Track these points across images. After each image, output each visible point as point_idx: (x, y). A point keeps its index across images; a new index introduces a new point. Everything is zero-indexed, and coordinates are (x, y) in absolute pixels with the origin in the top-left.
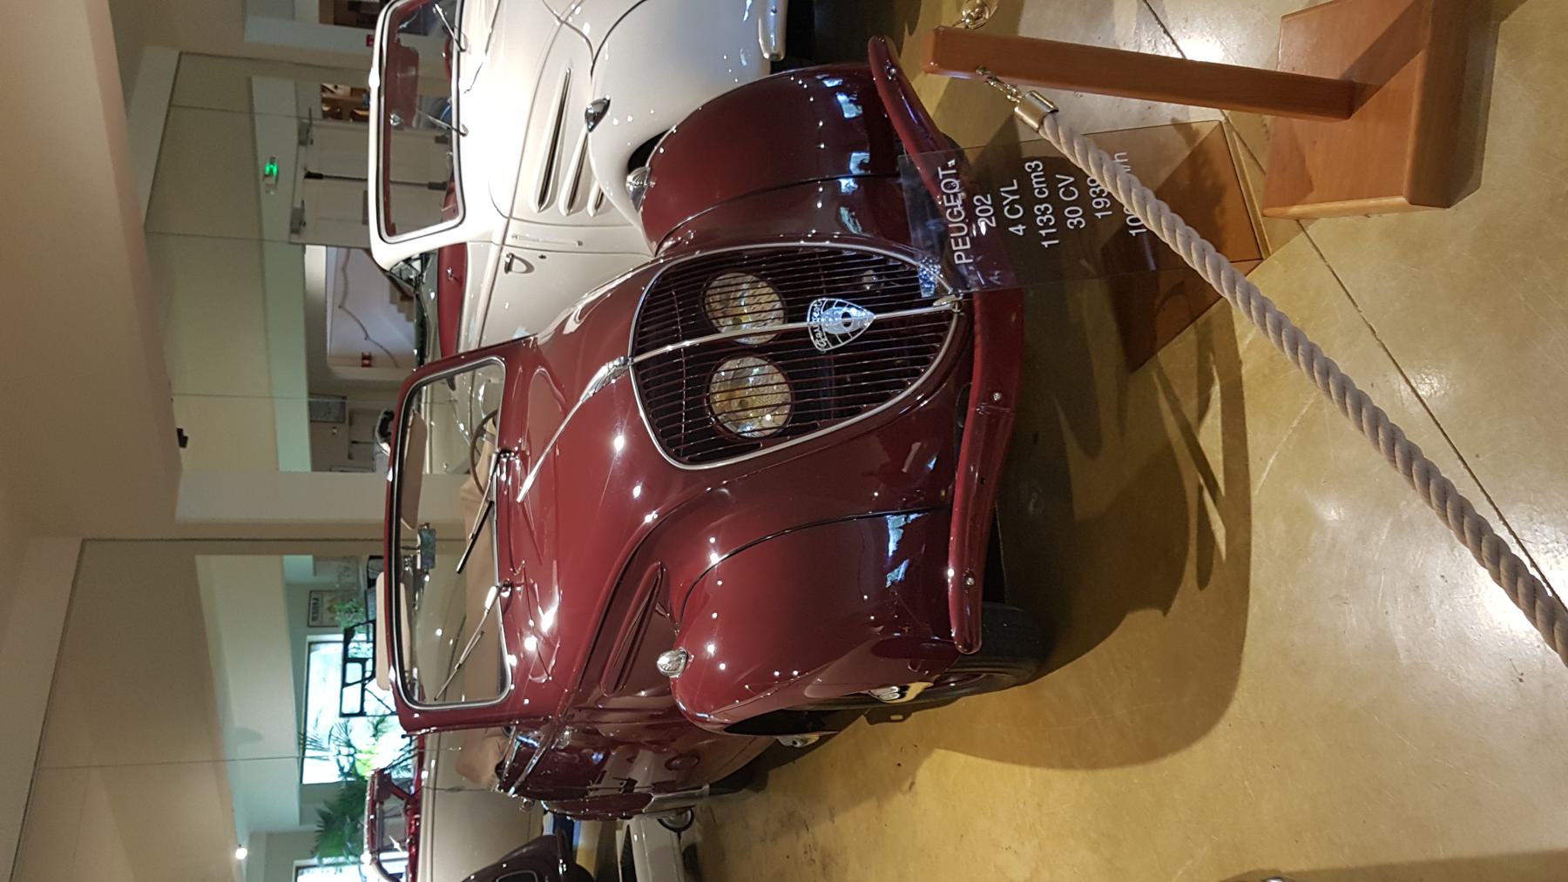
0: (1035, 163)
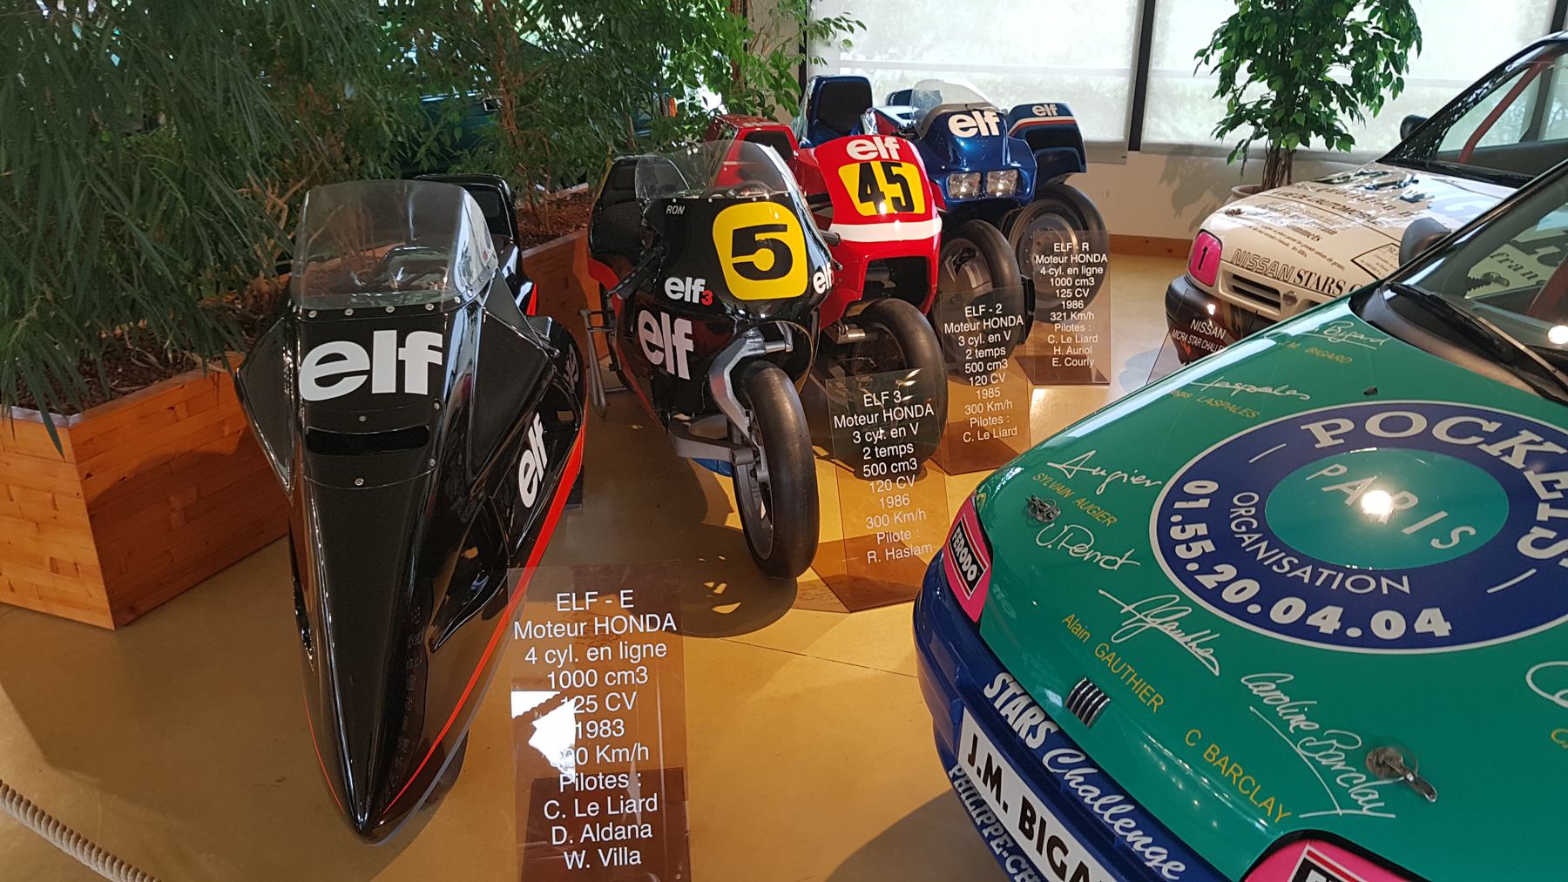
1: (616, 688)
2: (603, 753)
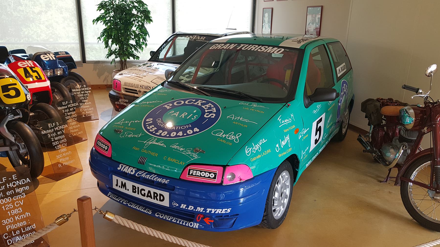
2: (17, 217)
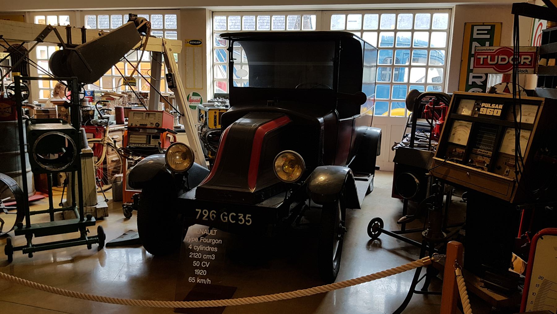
0: (214, 258)
1: (205, 260)
